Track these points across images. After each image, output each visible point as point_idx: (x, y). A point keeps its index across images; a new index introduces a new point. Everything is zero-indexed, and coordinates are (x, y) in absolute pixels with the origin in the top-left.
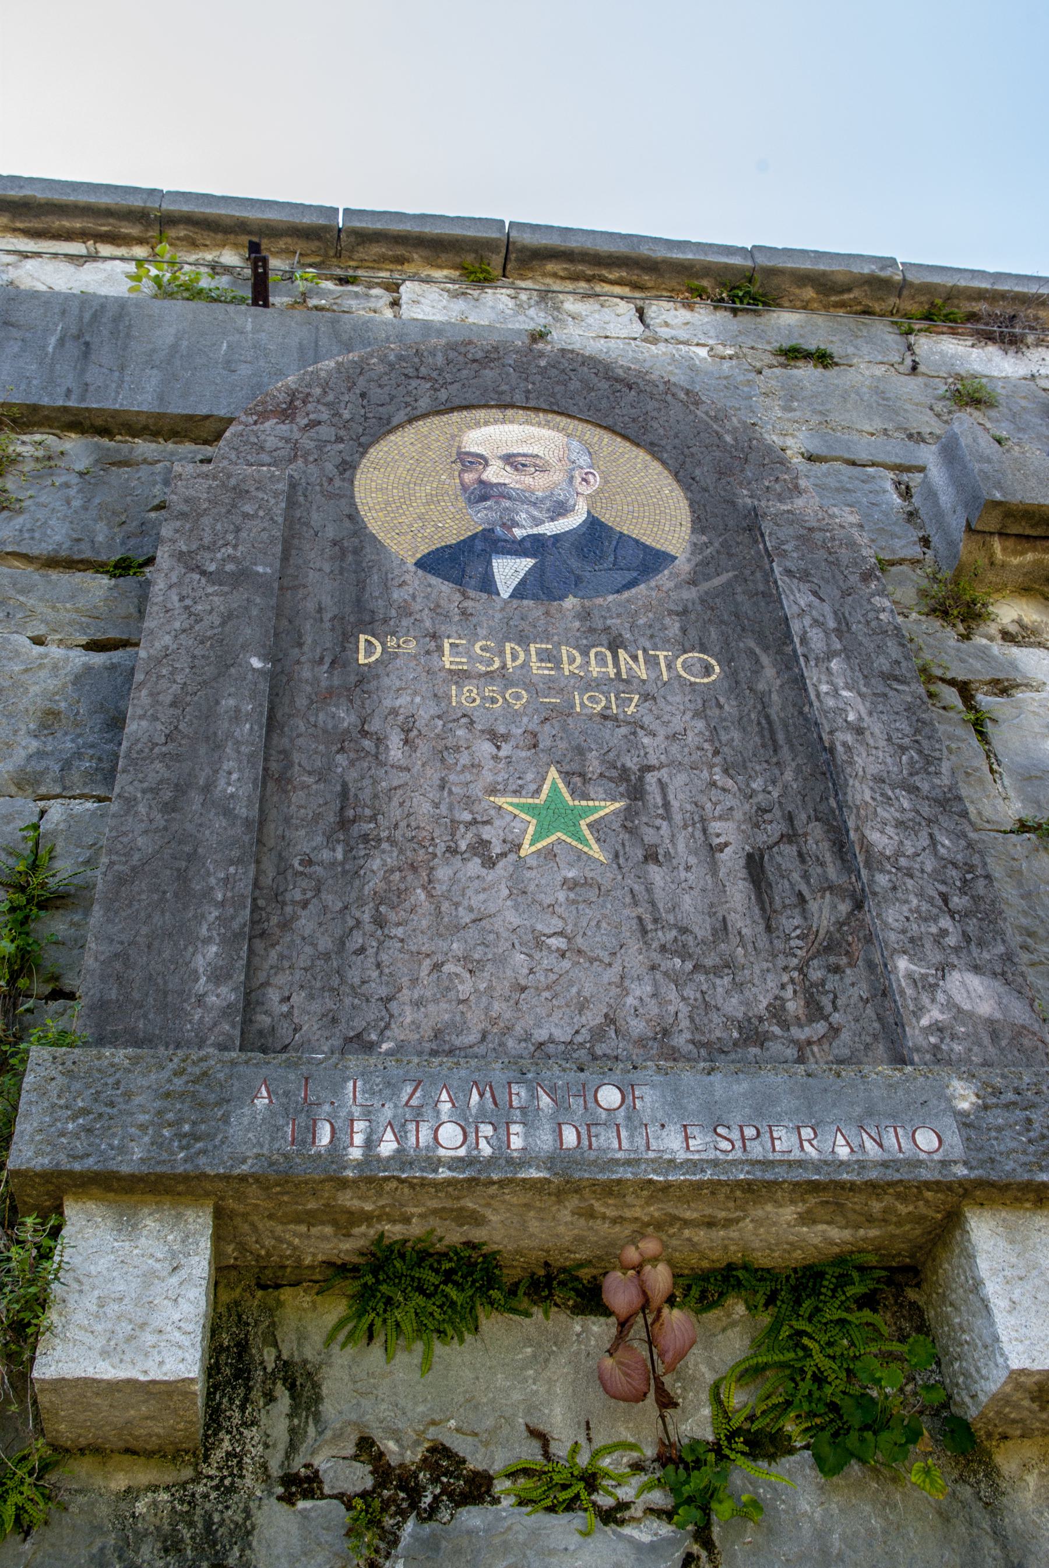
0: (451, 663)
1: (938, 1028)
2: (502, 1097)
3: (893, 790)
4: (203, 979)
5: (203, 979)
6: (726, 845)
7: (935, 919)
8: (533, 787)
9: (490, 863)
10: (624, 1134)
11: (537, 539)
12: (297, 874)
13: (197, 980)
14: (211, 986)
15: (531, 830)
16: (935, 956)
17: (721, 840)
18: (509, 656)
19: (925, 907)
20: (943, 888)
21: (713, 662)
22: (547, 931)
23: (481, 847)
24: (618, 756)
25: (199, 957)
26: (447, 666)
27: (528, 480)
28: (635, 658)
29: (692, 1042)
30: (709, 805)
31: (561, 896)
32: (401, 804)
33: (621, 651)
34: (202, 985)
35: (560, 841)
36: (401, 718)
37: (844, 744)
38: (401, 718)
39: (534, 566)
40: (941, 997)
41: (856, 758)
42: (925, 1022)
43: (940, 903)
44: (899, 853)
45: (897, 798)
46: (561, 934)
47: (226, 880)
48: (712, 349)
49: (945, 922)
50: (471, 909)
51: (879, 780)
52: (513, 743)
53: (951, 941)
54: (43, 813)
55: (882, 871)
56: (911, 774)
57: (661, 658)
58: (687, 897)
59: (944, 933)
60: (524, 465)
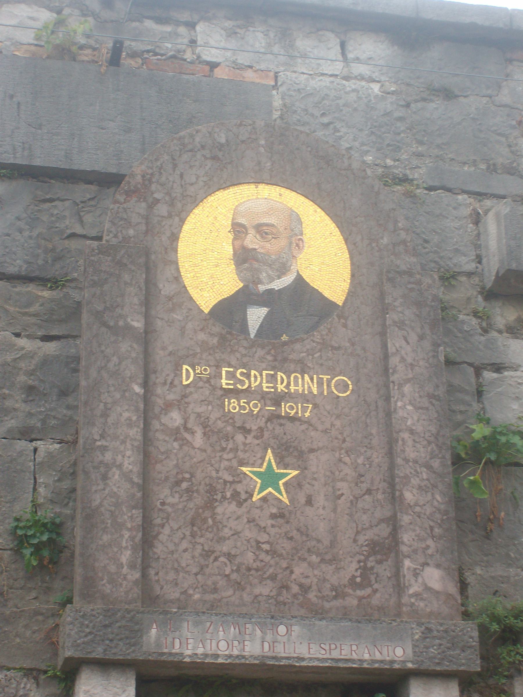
0: (227, 384)
1: (416, 595)
2: (242, 629)
3: (420, 467)
4: (126, 567)
5: (126, 567)
6: (342, 494)
7: (425, 540)
8: (260, 461)
9: (240, 504)
10: (286, 646)
11: (270, 292)
12: (160, 510)
13: (123, 568)
14: (129, 570)
15: (258, 485)
16: (422, 560)
17: (340, 492)
18: (253, 379)
19: (423, 533)
20: (432, 524)
21: (349, 383)
22: (262, 541)
23: (236, 494)
24: (299, 443)
25: (123, 556)
26: (225, 386)
27: (268, 245)
28: (312, 379)
29: (316, 596)
30: (337, 473)
31: (270, 522)
32: (202, 471)
33: (306, 375)
34: (125, 570)
35: (270, 493)
36: (202, 419)
37: (403, 440)
38: (202, 419)
39: (268, 312)
40: (420, 580)
41: (407, 449)
42: (411, 591)
43: (429, 531)
44: (416, 504)
45: (421, 473)
46: (267, 542)
47: (131, 517)
48: (382, 86)
49: (430, 542)
50: (231, 529)
51: (415, 462)
52: (253, 434)
53: (430, 552)
54: (35, 450)
55: (407, 514)
56: (431, 459)
57: (325, 379)
58: (322, 524)
59: (428, 547)
60: (266, 234)
